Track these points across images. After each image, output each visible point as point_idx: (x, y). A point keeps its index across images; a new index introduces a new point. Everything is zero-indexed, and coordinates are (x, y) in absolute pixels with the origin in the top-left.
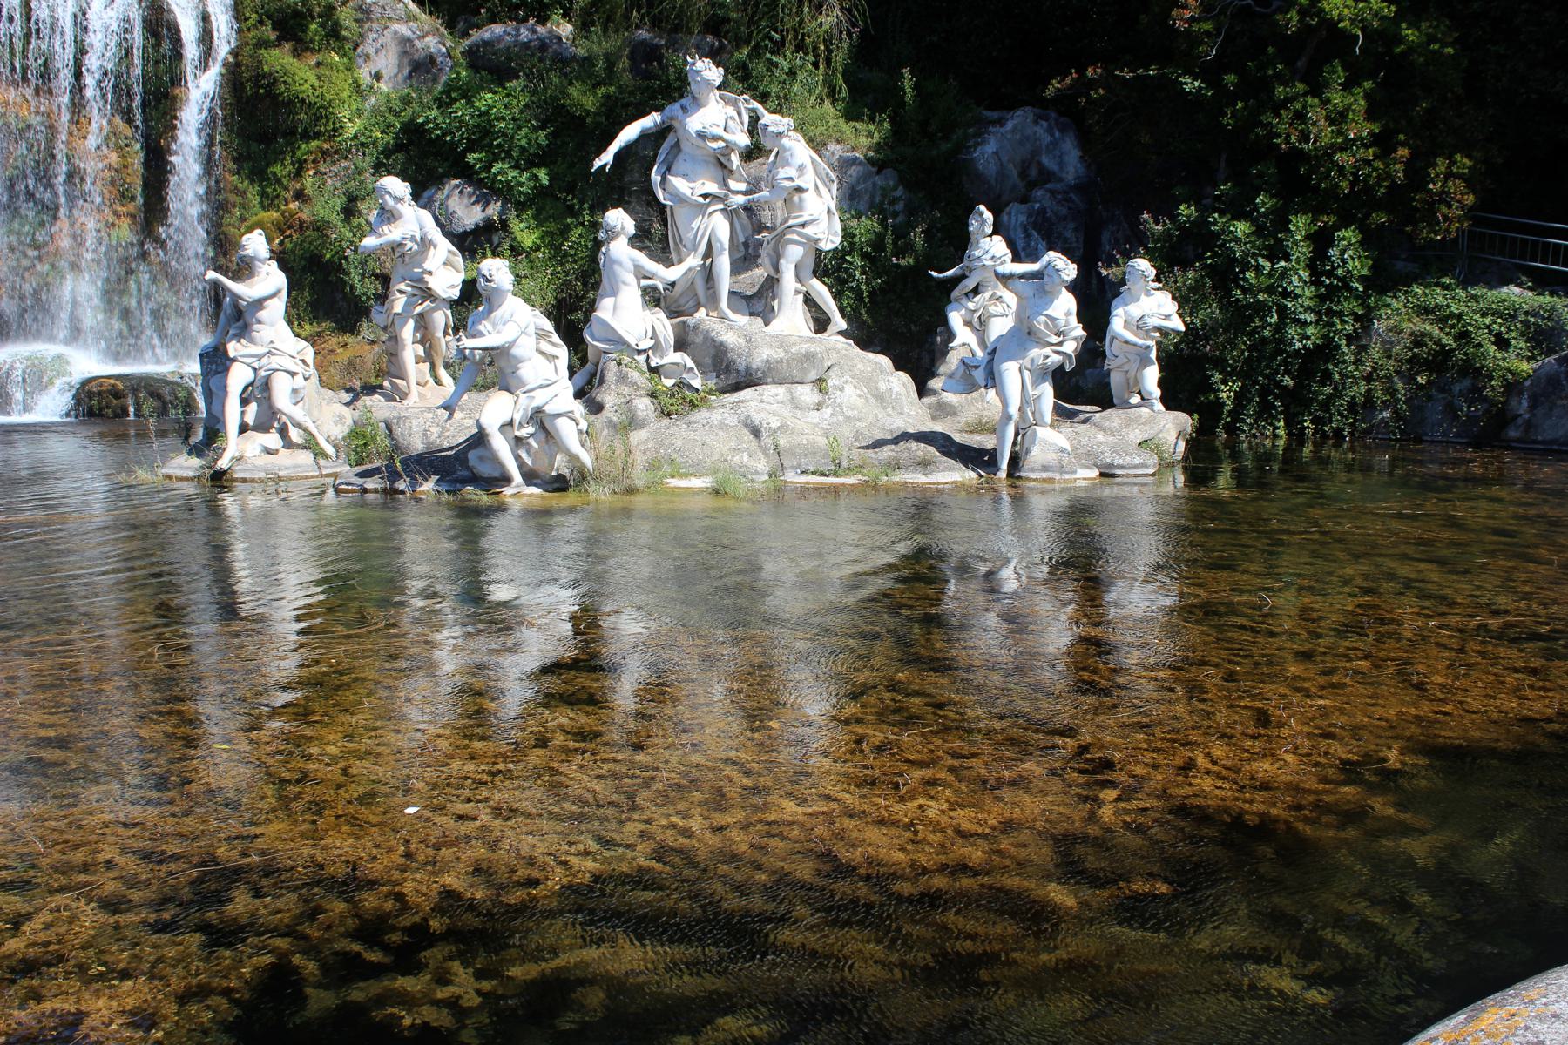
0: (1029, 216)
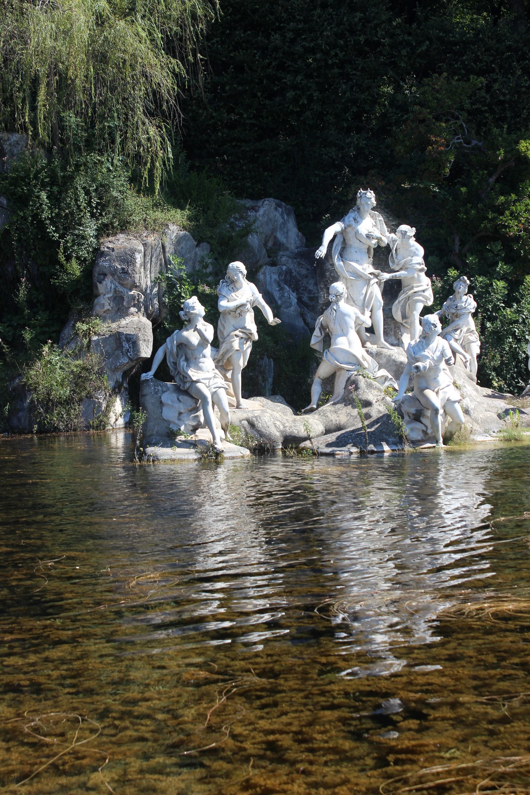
0: (280, 275)
